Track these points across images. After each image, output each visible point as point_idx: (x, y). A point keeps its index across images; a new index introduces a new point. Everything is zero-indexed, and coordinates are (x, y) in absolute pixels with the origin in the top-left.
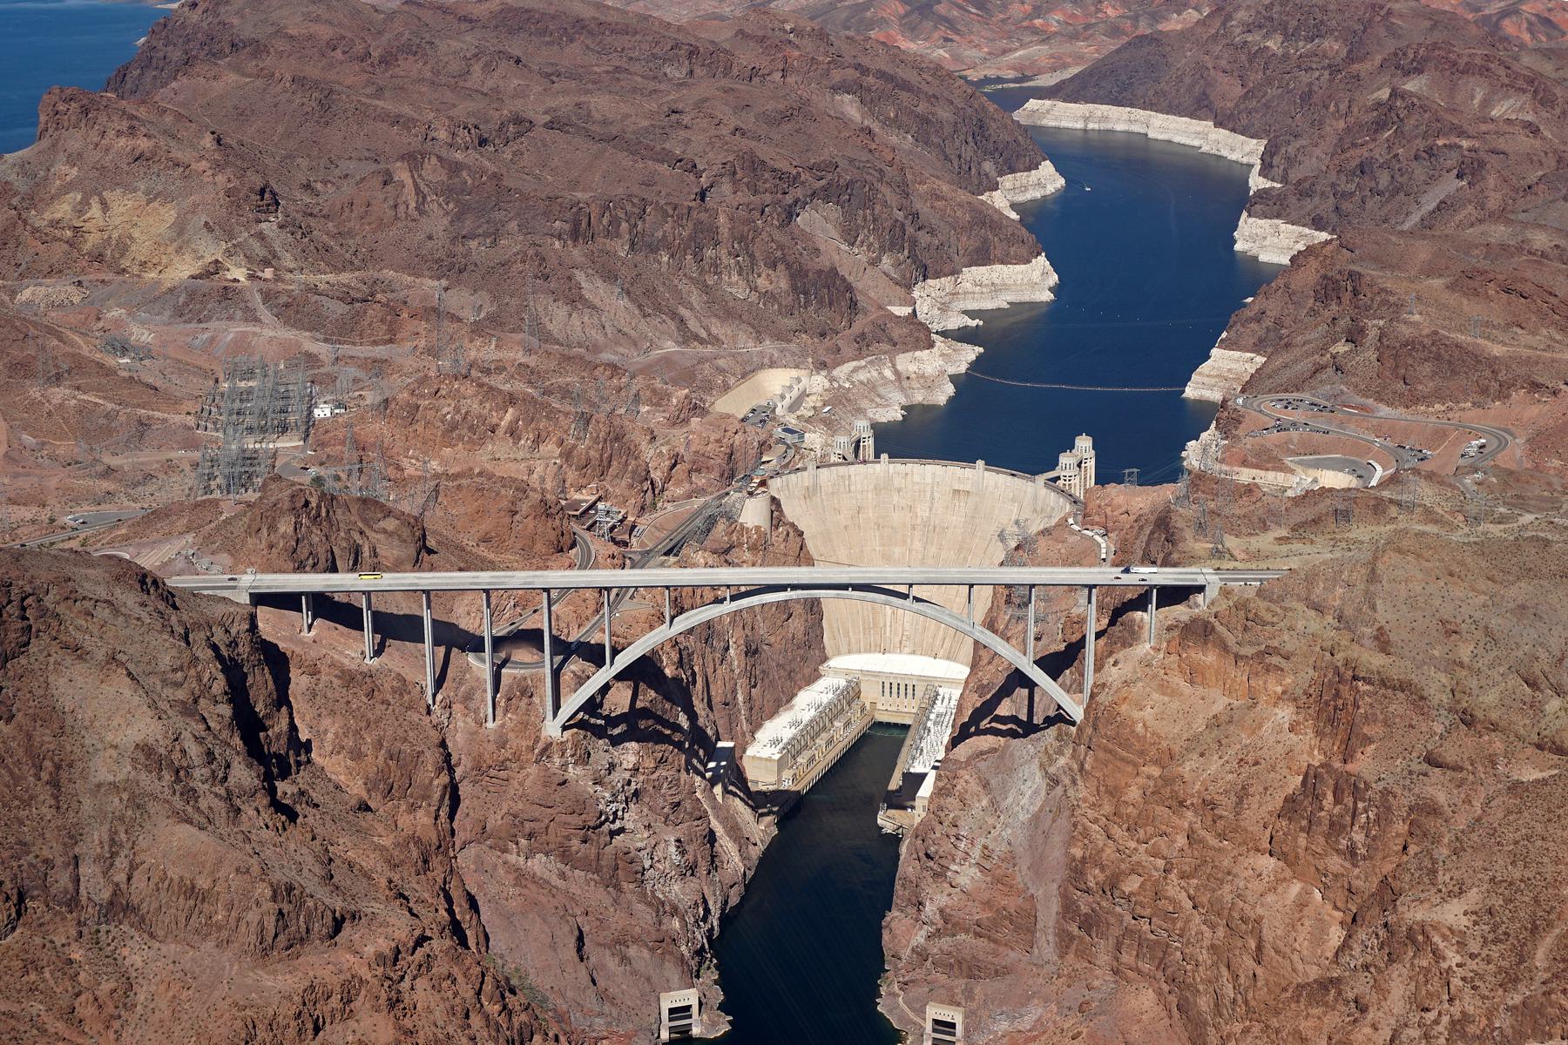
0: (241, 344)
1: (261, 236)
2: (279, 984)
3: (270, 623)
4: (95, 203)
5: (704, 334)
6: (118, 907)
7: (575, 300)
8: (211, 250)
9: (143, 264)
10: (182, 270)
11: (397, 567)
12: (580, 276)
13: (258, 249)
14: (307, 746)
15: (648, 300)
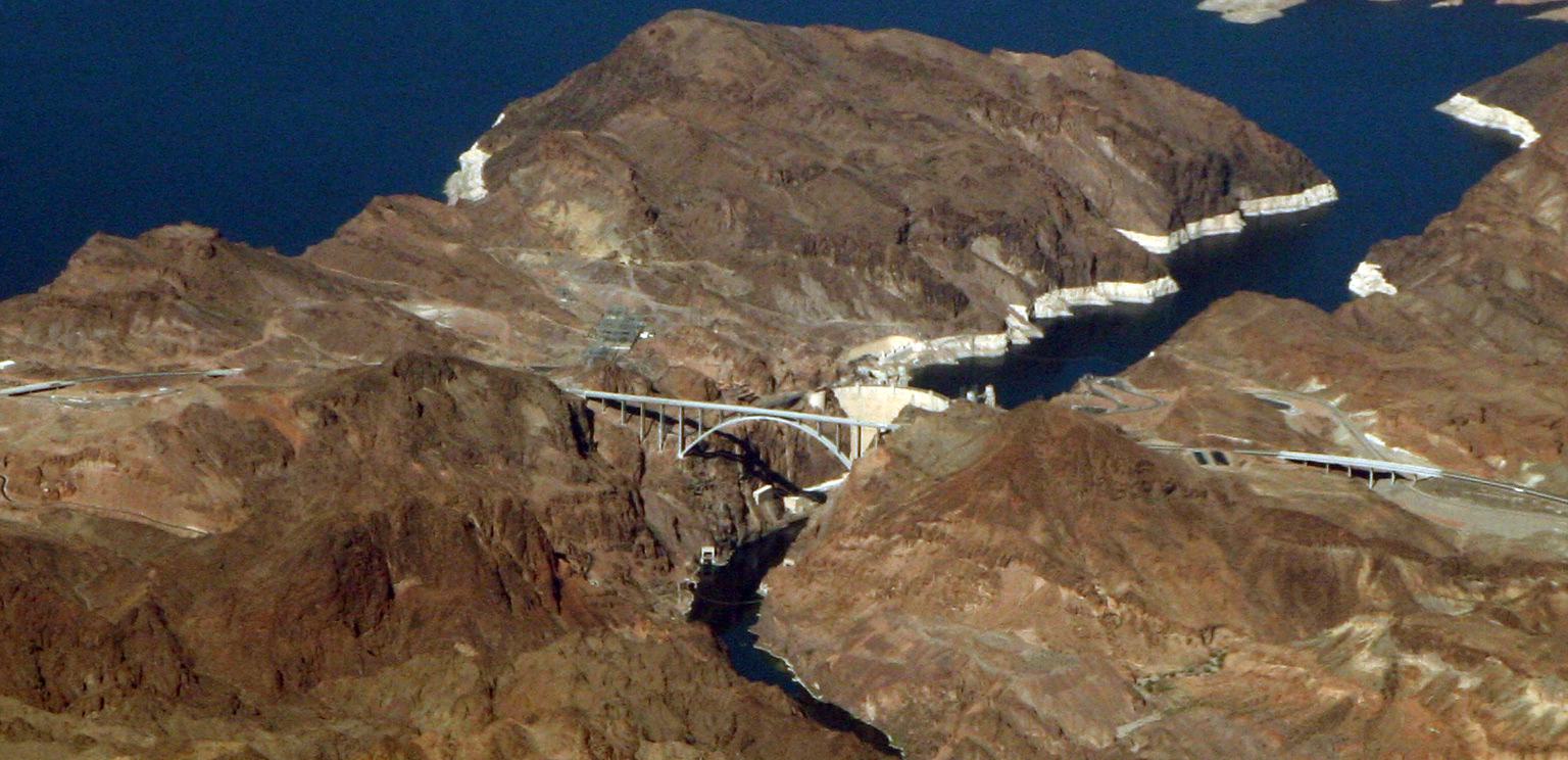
0: (618, 299)
1: (643, 239)
2: (570, 489)
3: (590, 405)
4: (562, 209)
5: (862, 313)
6: (533, 467)
7: (796, 289)
8: (615, 244)
9: (581, 247)
10: (599, 253)
11: (641, 395)
12: (802, 277)
13: (639, 245)
14: (596, 445)
15: (837, 291)
